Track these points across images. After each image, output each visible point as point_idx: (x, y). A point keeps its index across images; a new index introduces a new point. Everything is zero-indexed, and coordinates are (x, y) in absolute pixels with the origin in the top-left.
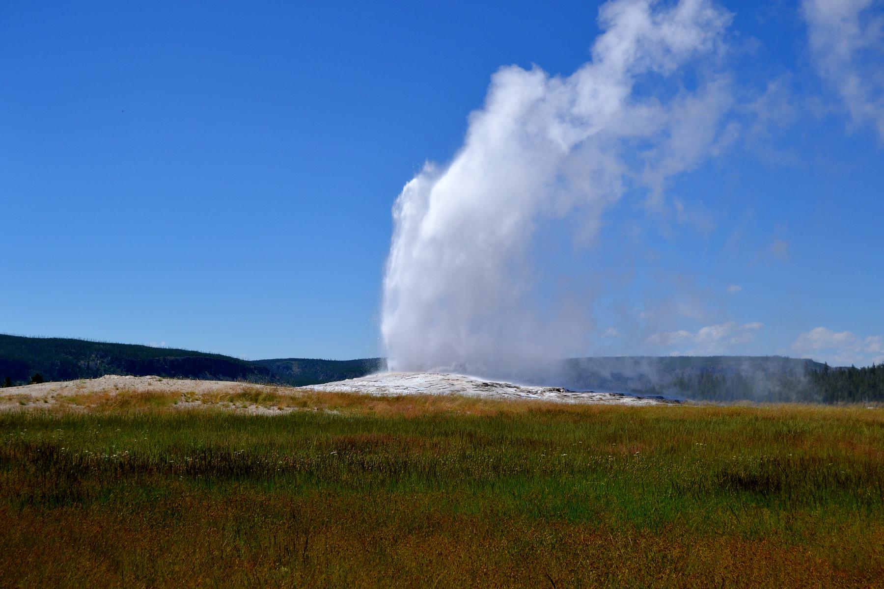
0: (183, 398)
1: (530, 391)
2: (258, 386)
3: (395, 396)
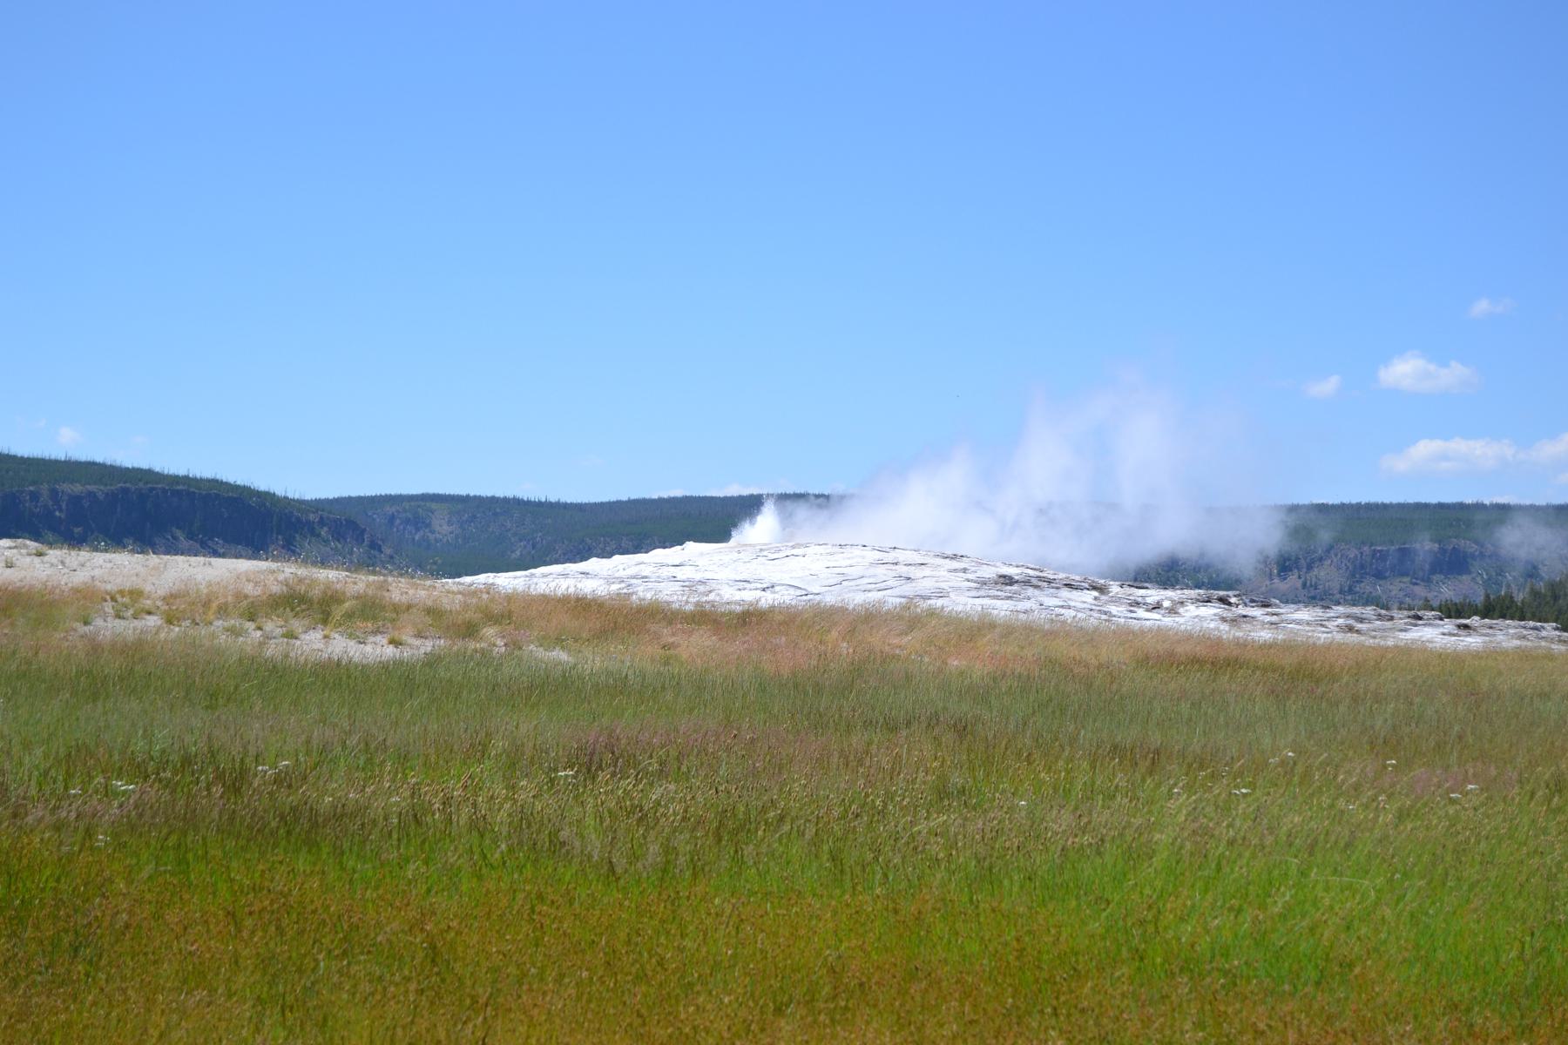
0: (108, 607)
1: (1140, 600)
2: (330, 576)
3: (738, 609)
